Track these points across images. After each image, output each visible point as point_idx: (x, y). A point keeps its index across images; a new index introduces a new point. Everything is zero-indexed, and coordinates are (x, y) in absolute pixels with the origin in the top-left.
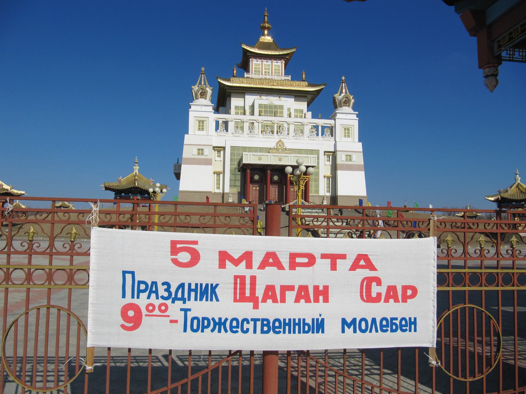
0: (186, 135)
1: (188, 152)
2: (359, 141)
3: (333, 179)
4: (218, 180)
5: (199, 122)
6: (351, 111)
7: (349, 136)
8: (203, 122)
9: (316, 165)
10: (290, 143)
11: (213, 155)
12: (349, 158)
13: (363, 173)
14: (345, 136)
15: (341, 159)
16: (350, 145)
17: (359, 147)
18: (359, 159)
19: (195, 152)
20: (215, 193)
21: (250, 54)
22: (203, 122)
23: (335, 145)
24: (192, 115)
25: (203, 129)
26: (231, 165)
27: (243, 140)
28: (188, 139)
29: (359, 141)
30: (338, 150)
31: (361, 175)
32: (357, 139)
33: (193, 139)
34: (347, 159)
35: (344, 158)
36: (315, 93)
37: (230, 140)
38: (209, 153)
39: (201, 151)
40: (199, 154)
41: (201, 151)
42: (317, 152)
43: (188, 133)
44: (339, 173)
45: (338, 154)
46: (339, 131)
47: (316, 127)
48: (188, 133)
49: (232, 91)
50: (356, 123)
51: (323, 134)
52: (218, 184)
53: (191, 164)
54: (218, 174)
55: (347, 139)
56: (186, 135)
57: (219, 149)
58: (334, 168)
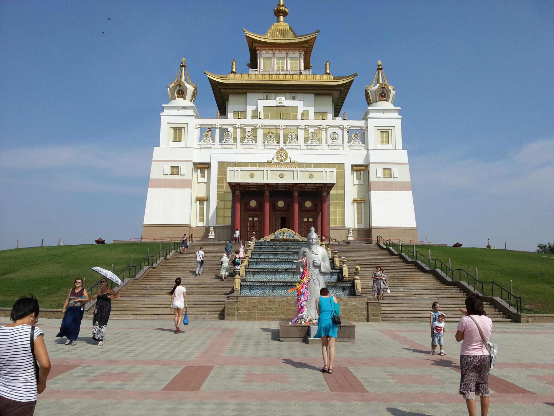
1: (158, 171)
3: (364, 203)
4: (202, 209)
5: (175, 129)
6: (392, 107)
8: (180, 129)
10: (299, 153)
11: (197, 177)
12: (388, 172)
15: (376, 174)
16: (389, 154)
17: (403, 156)
20: (197, 228)
21: (257, 45)
23: (367, 156)
24: (164, 120)
27: (237, 153)
28: (157, 153)
30: (371, 161)
31: (407, 197)
32: (399, 145)
33: (166, 153)
34: (384, 174)
35: (380, 173)
37: (215, 154)
38: (186, 170)
39: (175, 169)
40: (172, 173)
41: (175, 169)
42: (341, 166)
44: (375, 195)
45: (372, 168)
46: (373, 136)
49: (229, 91)
50: (398, 124)
52: (202, 215)
53: (161, 187)
54: (201, 200)
57: (203, 167)
58: (366, 187)
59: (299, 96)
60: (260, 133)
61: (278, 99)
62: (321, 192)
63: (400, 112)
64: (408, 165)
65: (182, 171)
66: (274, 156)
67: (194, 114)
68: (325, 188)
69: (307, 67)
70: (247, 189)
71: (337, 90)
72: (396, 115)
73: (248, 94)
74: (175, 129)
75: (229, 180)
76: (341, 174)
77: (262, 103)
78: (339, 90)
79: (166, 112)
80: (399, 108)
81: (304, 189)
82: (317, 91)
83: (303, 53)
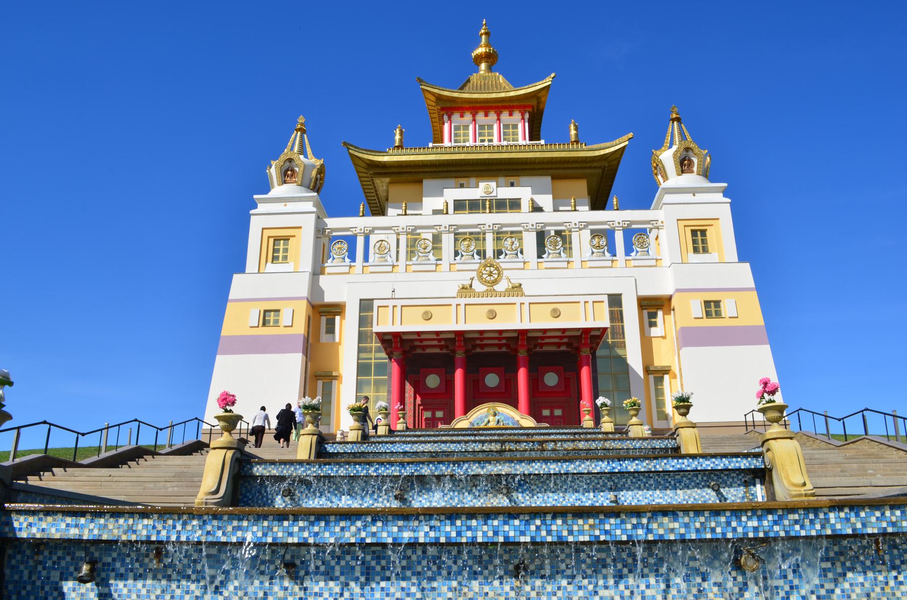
0: (236, 277)
1: (238, 320)
2: (742, 258)
7: (705, 250)
8: (286, 239)
9: (604, 322)
13: (768, 347)
14: (696, 250)
18: (743, 308)
19: (254, 318)
22: (286, 239)
24: (256, 224)
25: (285, 258)
26: (360, 350)
28: (240, 286)
29: (742, 258)
35: (697, 309)
36: (606, 164)
43: (242, 269)
47: (608, 235)
48: (242, 269)
51: (628, 250)
55: (701, 257)
56: (236, 277)
59: (523, 179)
60: (448, 241)
61: (482, 185)
62: (578, 350)
63: (726, 193)
64: (755, 293)
65: (285, 318)
66: (474, 274)
67: (315, 209)
68: (586, 338)
69: (534, 135)
70: (419, 351)
71: (595, 167)
72: (719, 197)
73: (426, 182)
74: (277, 240)
75: (376, 329)
76: (617, 316)
77: (453, 194)
78: (600, 167)
79: (261, 208)
80: (726, 185)
81: (542, 345)
82: (557, 171)
83: (527, 116)
